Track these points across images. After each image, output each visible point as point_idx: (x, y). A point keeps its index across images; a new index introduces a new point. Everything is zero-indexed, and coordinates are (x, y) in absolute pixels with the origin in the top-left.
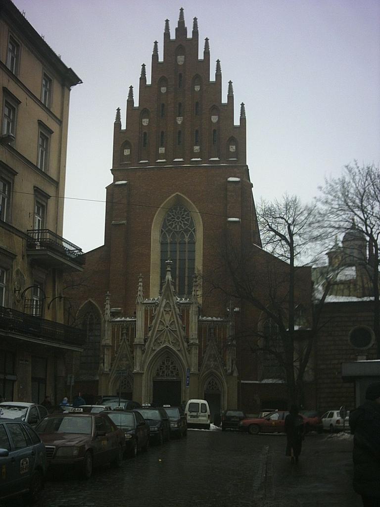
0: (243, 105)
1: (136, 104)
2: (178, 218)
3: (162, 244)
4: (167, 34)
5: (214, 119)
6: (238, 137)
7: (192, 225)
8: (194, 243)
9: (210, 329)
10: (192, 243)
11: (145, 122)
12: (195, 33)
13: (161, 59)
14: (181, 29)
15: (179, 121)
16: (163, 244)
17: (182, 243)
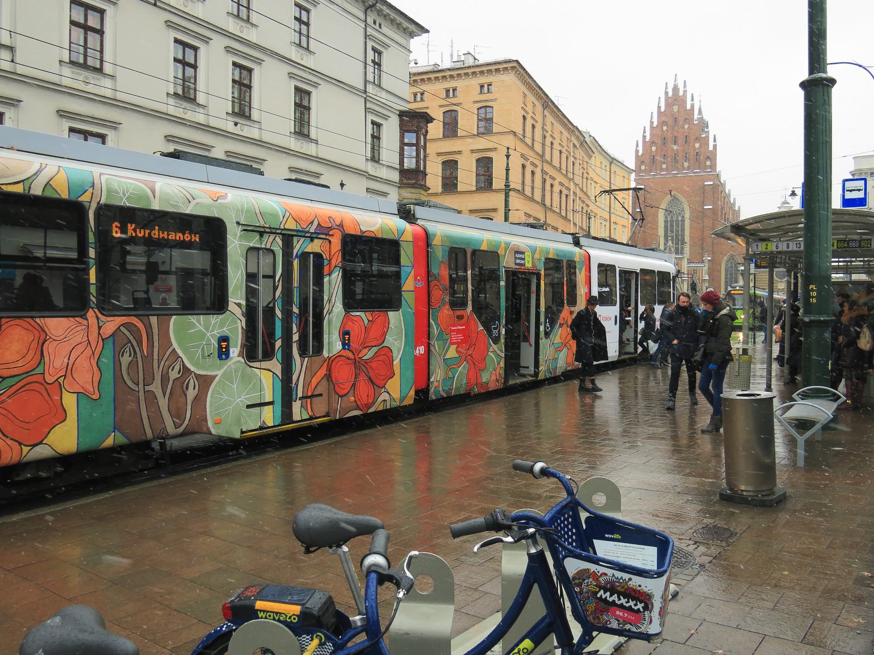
0: (715, 136)
1: (648, 139)
2: (675, 206)
3: (665, 221)
4: (666, 93)
5: (697, 145)
6: (712, 157)
7: (683, 210)
8: (684, 220)
9: (694, 270)
10: (683, 221)
11: (654, 149)
12: (685, 92)
13: (663, 109)
14: (676, 89)
15: (675, 147)
16: (666, 222)
17: (677, 221)
